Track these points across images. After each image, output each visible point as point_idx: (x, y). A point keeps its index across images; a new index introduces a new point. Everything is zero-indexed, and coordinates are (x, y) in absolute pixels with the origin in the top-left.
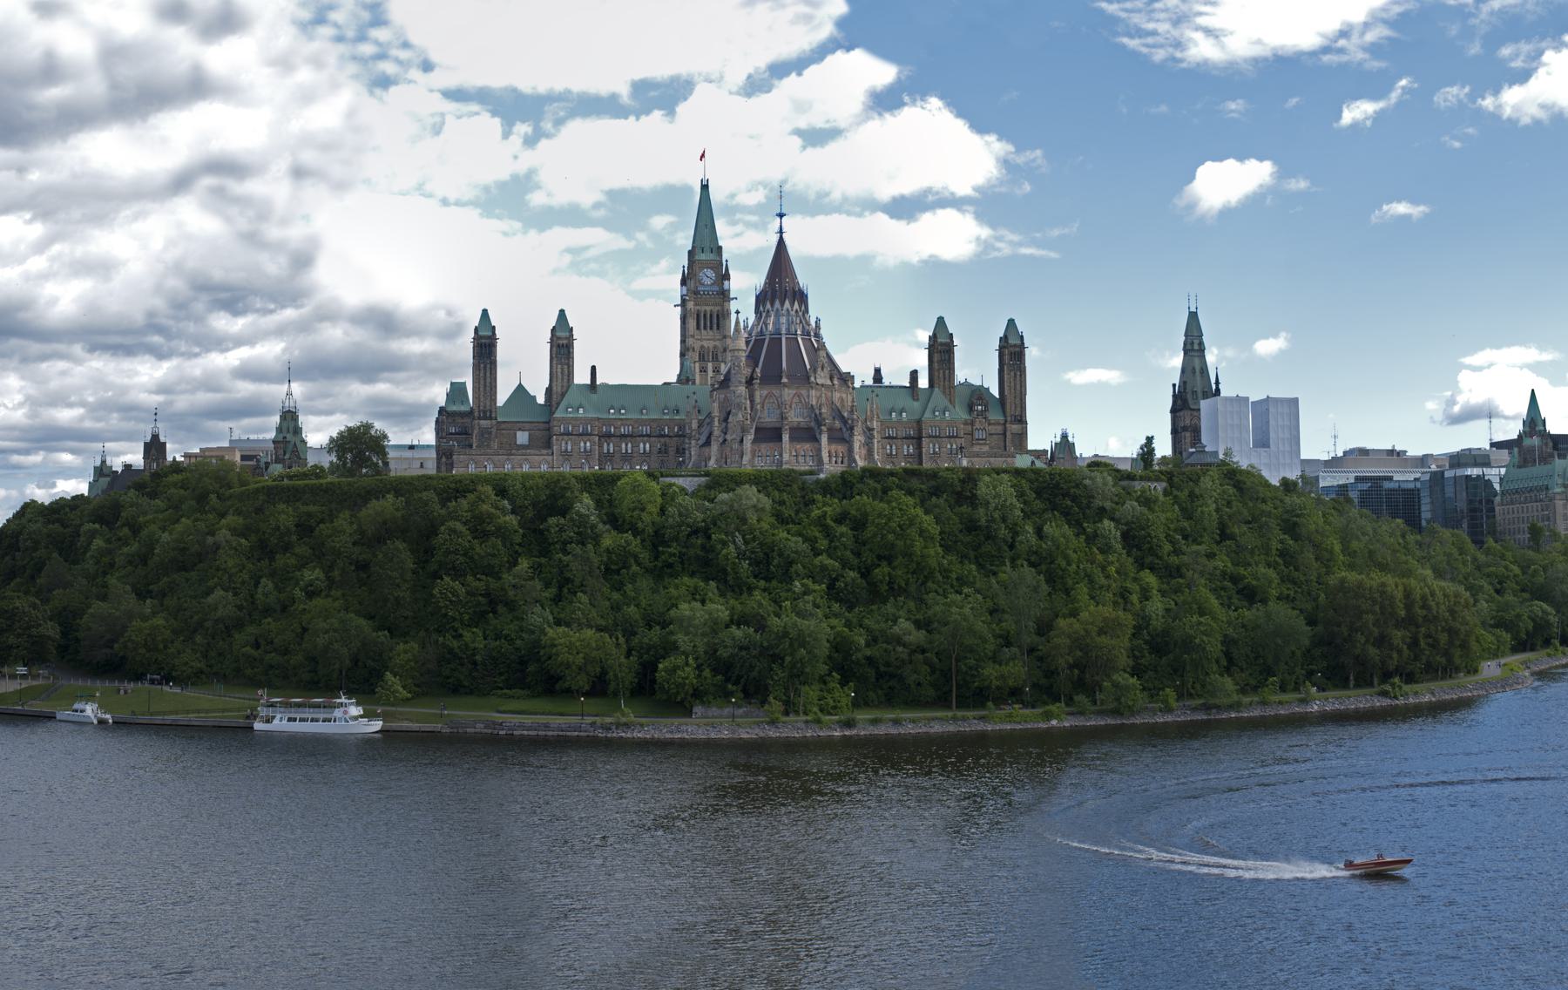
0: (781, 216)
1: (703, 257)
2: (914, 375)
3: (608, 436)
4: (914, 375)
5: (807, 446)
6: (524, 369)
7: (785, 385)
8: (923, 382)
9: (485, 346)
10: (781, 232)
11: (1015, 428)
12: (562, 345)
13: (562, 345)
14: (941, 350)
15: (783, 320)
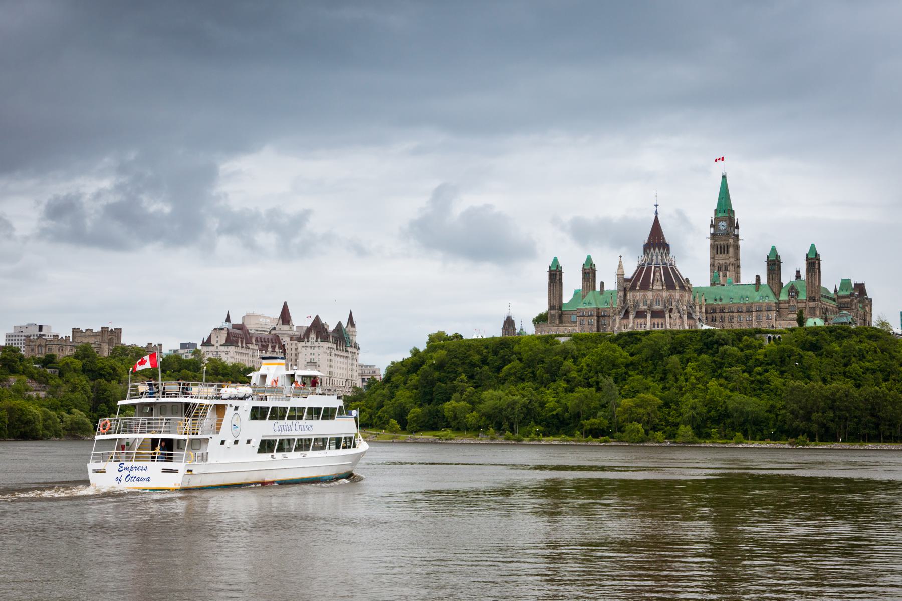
0: (656, 206)
1: (720, 215)
2: (758, 278)
3: (604, 316)
4: (758, 278)
5: (642, 320)
6: (572, 283)
7: (639, 291)
8: (764, 281)
9: (555, 276)
10: (656, 213)
11: (812, 304)
12: (589, 273)
13: (589, 273)
14: (774, 264)
15: (654, 258)
